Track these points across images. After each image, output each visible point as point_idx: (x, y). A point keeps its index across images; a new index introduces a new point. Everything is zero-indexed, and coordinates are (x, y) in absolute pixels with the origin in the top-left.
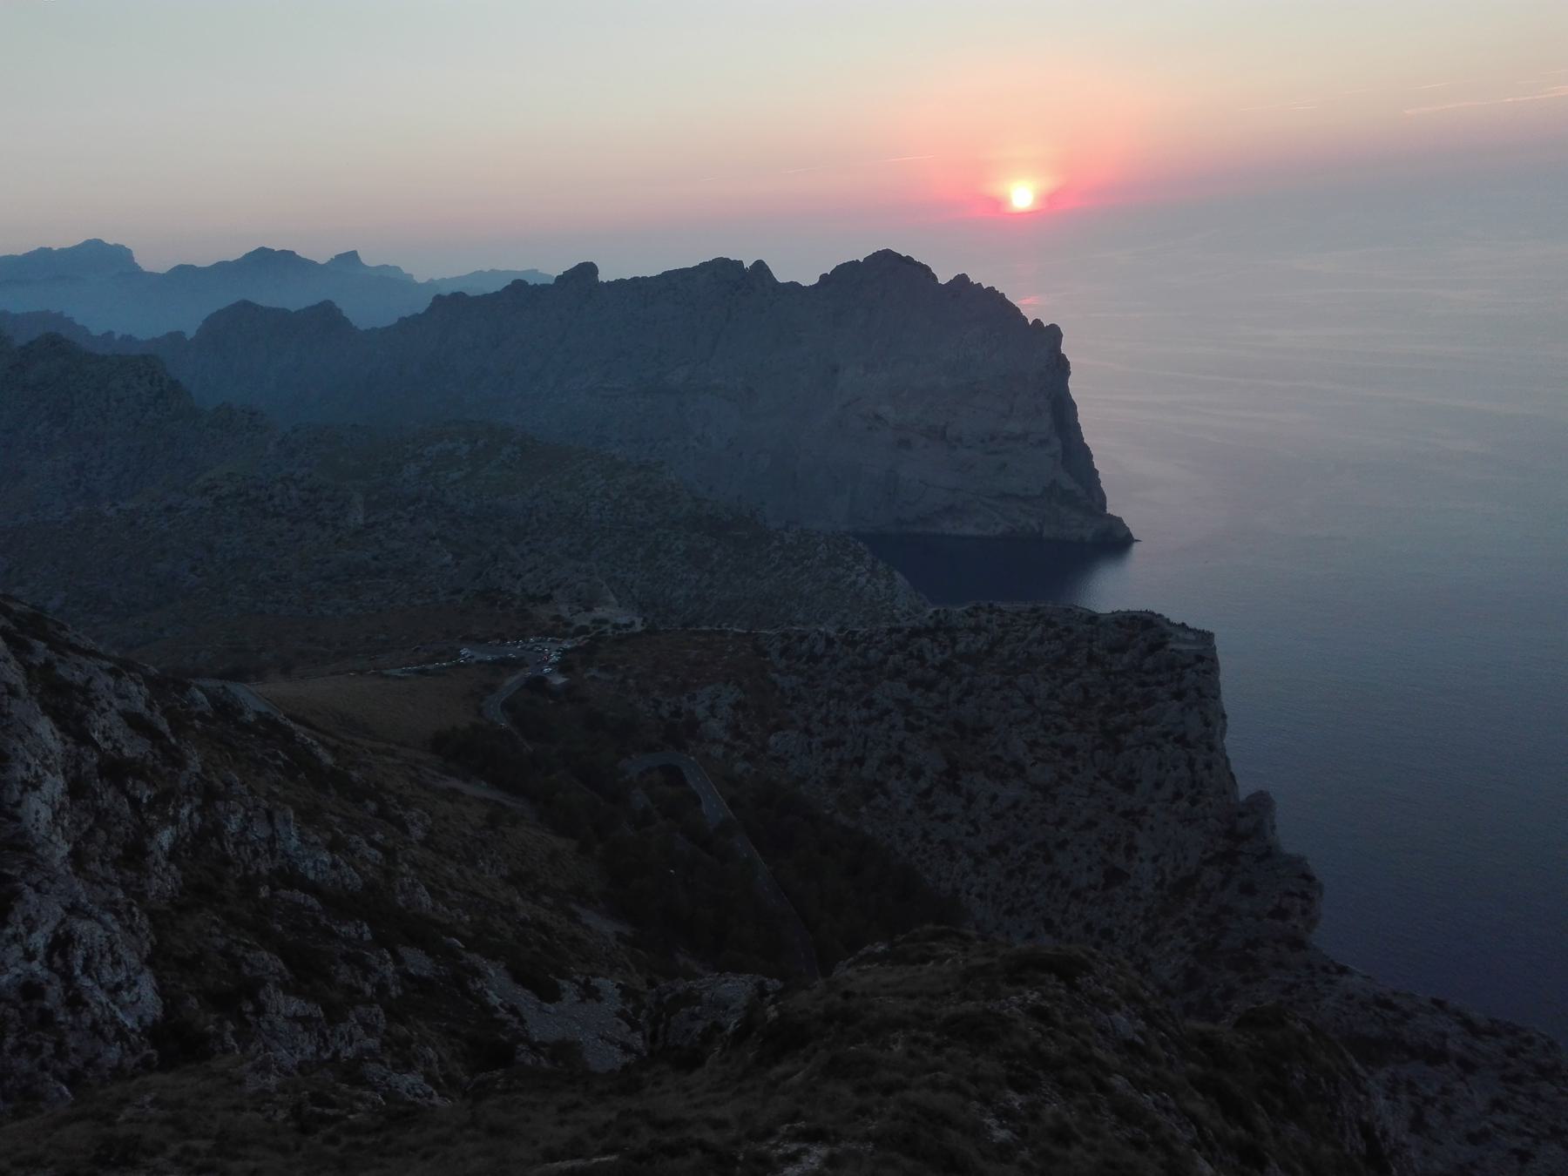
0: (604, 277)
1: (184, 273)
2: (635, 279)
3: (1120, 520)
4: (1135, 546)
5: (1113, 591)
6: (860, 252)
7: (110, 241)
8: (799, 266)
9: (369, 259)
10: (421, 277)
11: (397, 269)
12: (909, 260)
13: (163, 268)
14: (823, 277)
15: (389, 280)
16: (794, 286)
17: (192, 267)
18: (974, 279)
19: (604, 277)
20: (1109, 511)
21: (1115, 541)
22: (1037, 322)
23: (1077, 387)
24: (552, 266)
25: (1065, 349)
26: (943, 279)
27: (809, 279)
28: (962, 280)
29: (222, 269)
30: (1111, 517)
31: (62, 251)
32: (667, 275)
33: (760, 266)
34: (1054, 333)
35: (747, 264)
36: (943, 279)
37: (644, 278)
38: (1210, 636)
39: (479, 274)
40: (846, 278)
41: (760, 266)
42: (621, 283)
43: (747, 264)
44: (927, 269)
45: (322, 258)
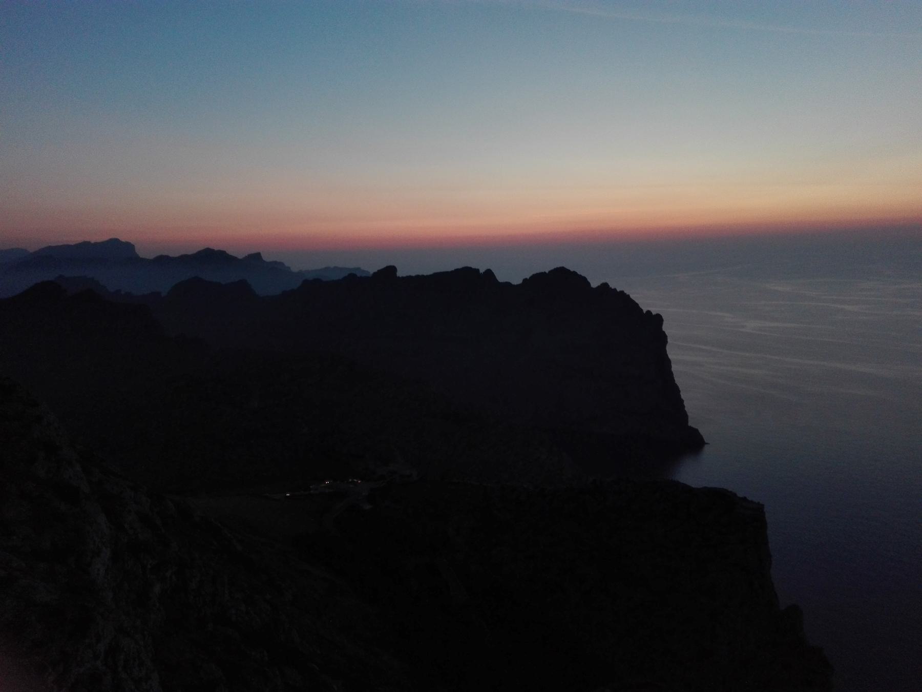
0: (400, 274)
1: (163, 261)
2: (418, 277)
3: (696, 431)
4: (706, 448)
5: (694, 474)
6: (547, 267)
7: (123, 239)
8: (512, 274)
9: (267, 258)
10: (295, 269)
11: (282, 264)
12: (575, 273)
13: (151, 256)
14: (525, 280)
15: (276, 268)
16: (508, 284)
17: (167, 257)
18: (612, 286)
19: (400, 274)
20: (690, 424)
21: (693, 442)
22: (649, 312)
23: (672, 353)
24: (372, 267)
25: (664, 328)
26: (594, 284)
27: (517, 281)
28: (605, 286)
29: (185, 259)
30: (691, 428)
31: (96, 244)
32: (436, 275)
33: (489, 272)
34: (659, 319)
35: (482, 271)
36: (594, 284)
37: (423, 276)
38: (763, 505)
39: (327, 269)
40: (538, 280)
41: (489, 272)
42: (409, 278)
43: (482, 271)
44: (584, 279)
45: (240, 257)
